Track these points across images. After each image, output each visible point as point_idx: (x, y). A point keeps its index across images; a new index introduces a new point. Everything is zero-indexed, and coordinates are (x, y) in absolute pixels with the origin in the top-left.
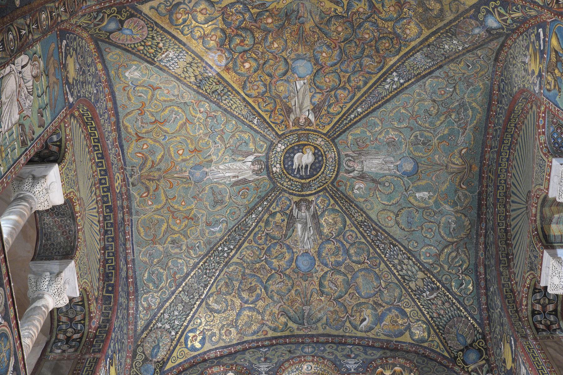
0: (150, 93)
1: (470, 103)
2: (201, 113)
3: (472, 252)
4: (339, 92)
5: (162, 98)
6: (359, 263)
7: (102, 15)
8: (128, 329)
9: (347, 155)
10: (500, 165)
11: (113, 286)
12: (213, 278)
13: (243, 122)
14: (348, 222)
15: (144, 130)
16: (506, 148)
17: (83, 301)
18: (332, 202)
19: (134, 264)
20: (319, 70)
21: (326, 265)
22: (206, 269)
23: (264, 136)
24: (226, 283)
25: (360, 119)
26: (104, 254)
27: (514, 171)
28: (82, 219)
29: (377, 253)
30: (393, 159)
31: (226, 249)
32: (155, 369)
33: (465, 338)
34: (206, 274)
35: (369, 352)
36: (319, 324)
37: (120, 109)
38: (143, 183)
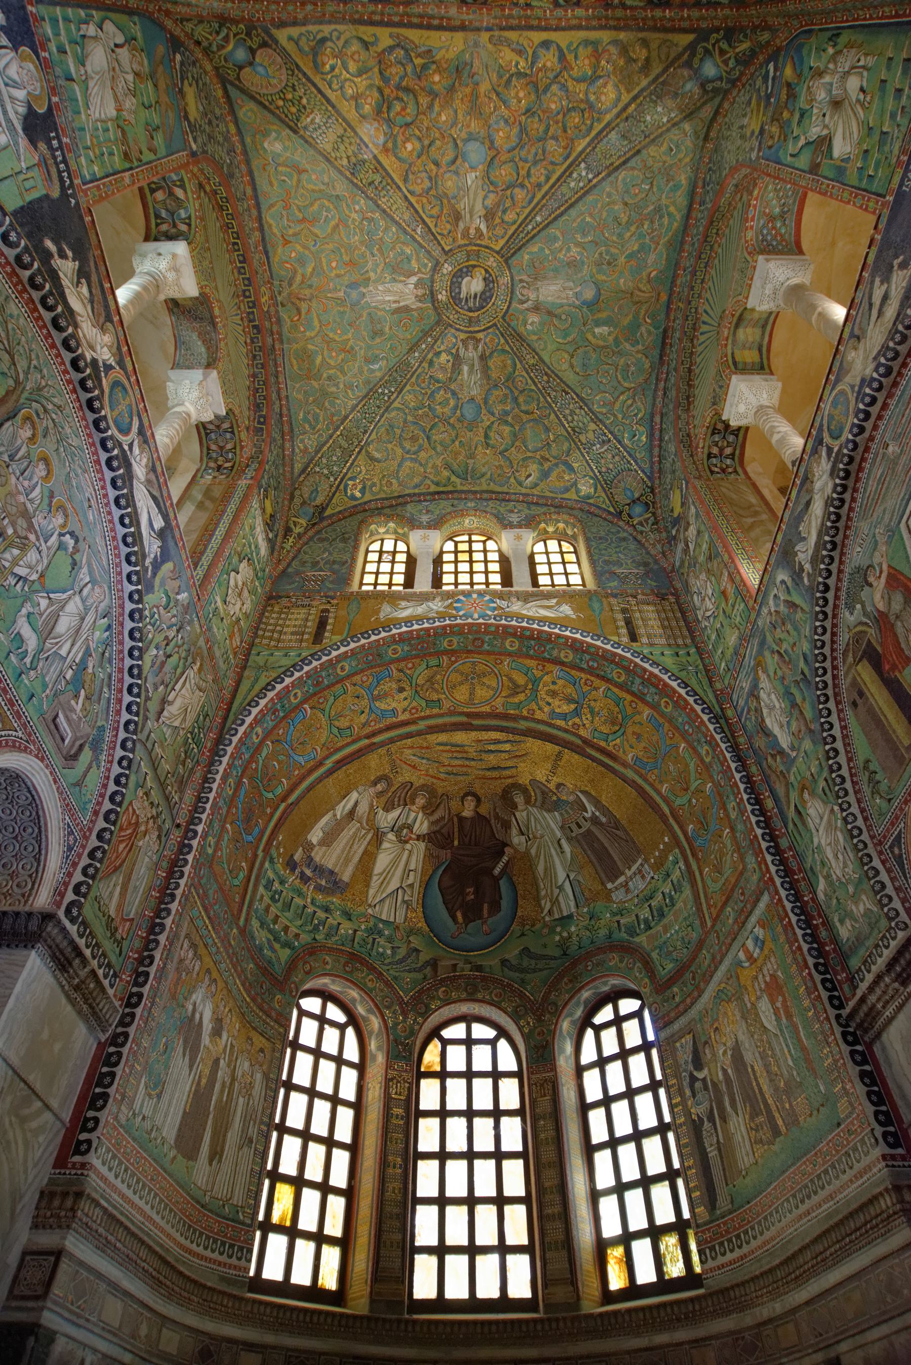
1: (667, 207)
3: (650, 399)
4: (517, 190)
5: (310, 187)
6: (527, 412)
9: (521, 281)
10: (692, 288)
11: (264, 417)
13: (405, 232)
14: (519, 366)
15: (291, 232)
16: (702, 265)
17: (232, 427)
18: (502, 341)
19: (288, 401)
20: (494, 157)
21: (493, 414)
23: (428, 252)
25: (539, 232)
27: (708, 296)
28: (224, 326)
29: (547, 402)
30: (571, 284)
33: (632, 492)
35: (533, 507)
36: (483, 480)
37: (261, 199)
38: (293, 303)
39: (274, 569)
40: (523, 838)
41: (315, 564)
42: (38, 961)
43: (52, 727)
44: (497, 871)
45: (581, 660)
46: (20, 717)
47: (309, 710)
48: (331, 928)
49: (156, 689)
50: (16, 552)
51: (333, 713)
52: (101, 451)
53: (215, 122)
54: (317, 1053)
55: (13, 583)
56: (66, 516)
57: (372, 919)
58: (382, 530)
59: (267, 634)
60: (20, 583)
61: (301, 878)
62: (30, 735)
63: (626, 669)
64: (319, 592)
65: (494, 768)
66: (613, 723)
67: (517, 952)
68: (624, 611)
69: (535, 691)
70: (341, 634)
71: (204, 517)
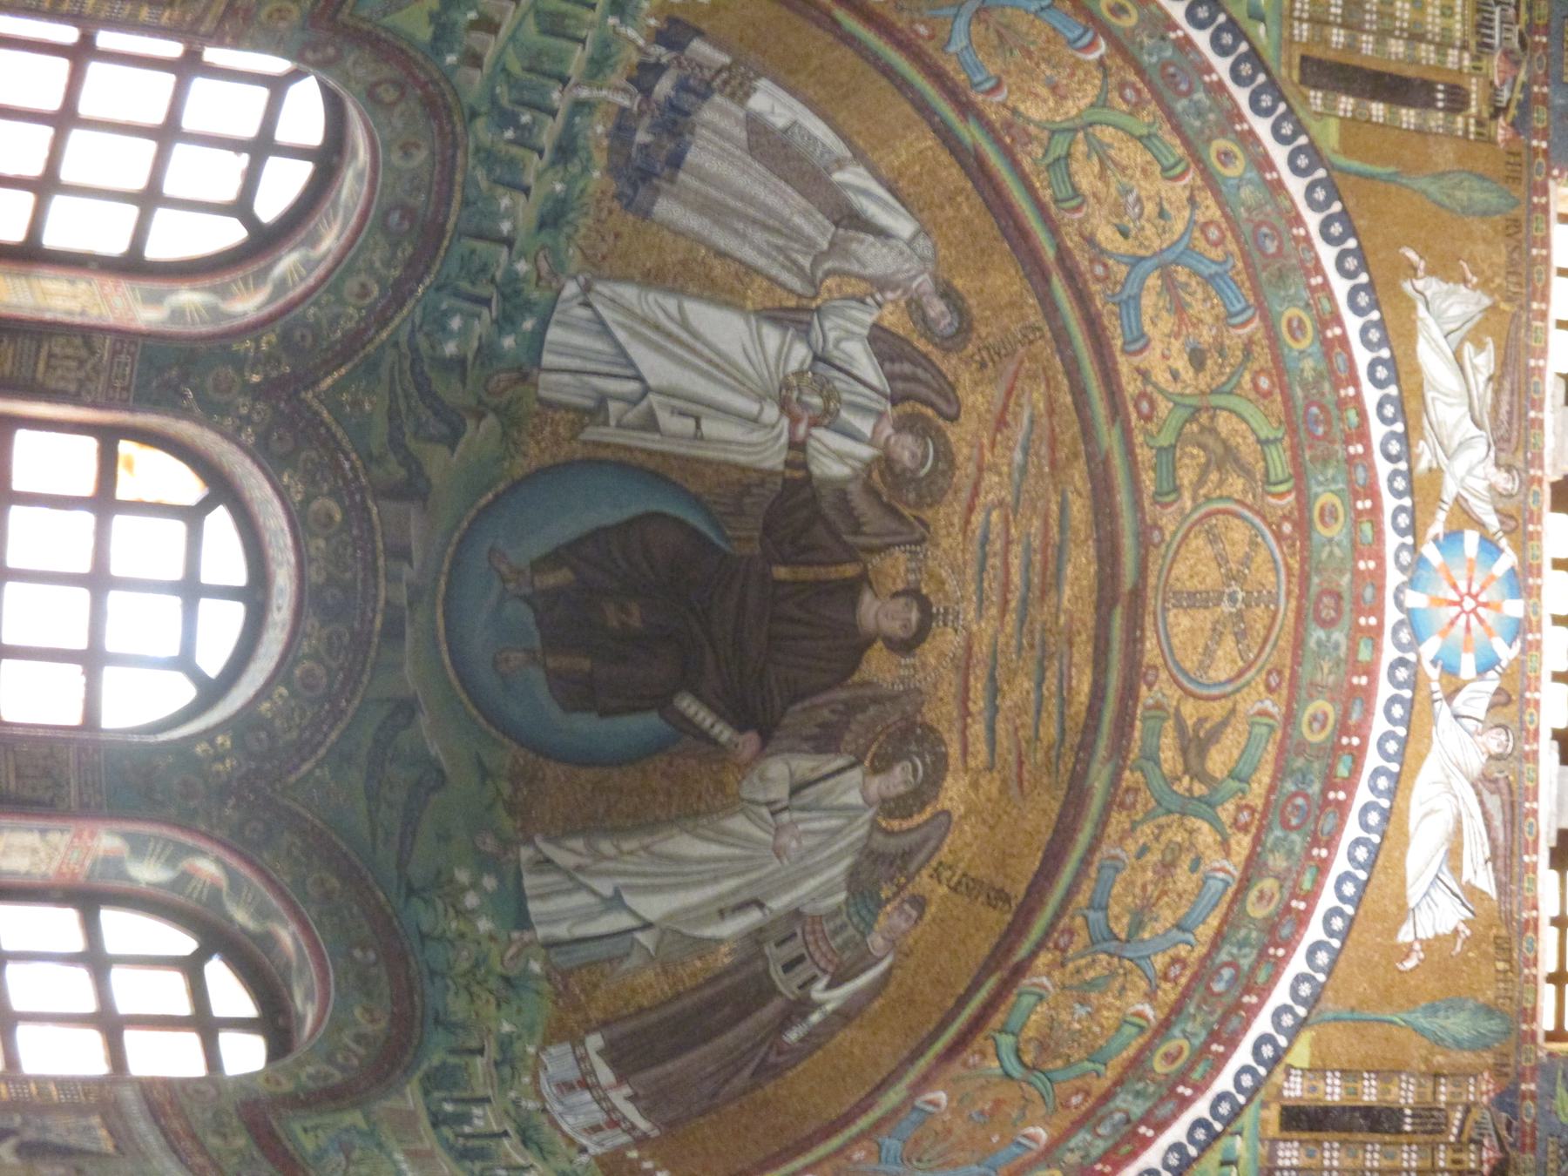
40: (780, 792)
44: (688, 704)
45: (1241, 945)
47: (1093, 56)
48: (512, 163)
51: (1106, 134)
54: (168, 133)
57: (549, 294)
61: (643, 66)
63: (1183, 1078)
65: (994, 691)
66: (1043, 1047)
67: (435, 750)
68: (1430, 1120)
69: (1186, 807)
70: (1346, 150)
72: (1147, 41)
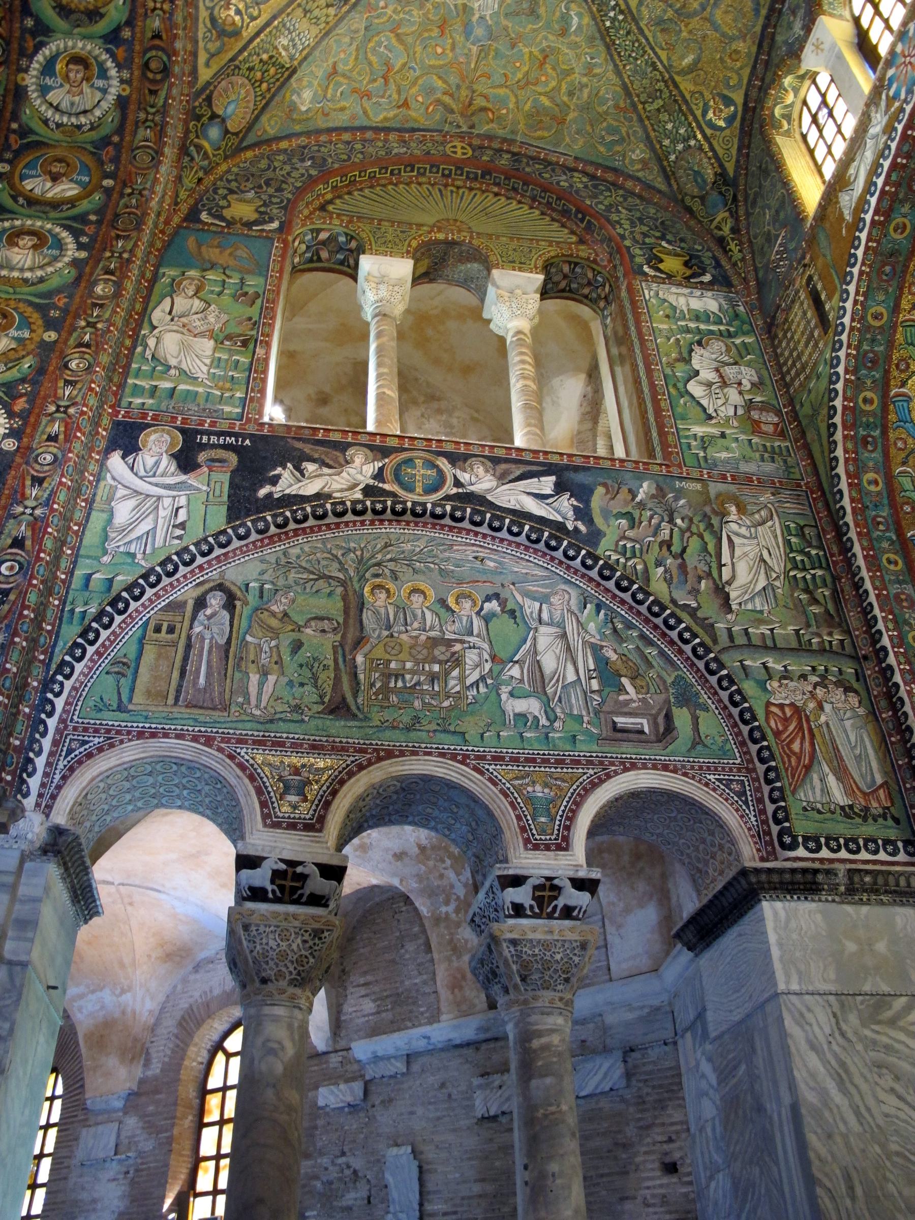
0: (341, 79)
2: (386, 7)
7: (192, 148)
8: (655, 204)
11: (578, 211)
12: (647, 48)
15: (395, 96)
17: (570, 263)
22: (630, 56)
24: (663, 30)
26: (540, 203)
31: (612, 14)
32: (720, 193)
34: (636, 59)
37: (357, 123)
38: (473, 114)
39: (748, 296)
41: (770, 239)
42: (778, 905)
43: (619, 735)
46: (578, 762)
49: (695, 592)
50: (455, 673)
52: (443, 522)
53: (269, 174)
55: (475, 692)
56: (469, 596)
58: (790, 99)
59: (793, 372)
60: (481, 685)
62: (601, 763)
64: (791, 266)
71: (628, 367)
72: (869, 382)
